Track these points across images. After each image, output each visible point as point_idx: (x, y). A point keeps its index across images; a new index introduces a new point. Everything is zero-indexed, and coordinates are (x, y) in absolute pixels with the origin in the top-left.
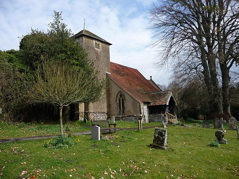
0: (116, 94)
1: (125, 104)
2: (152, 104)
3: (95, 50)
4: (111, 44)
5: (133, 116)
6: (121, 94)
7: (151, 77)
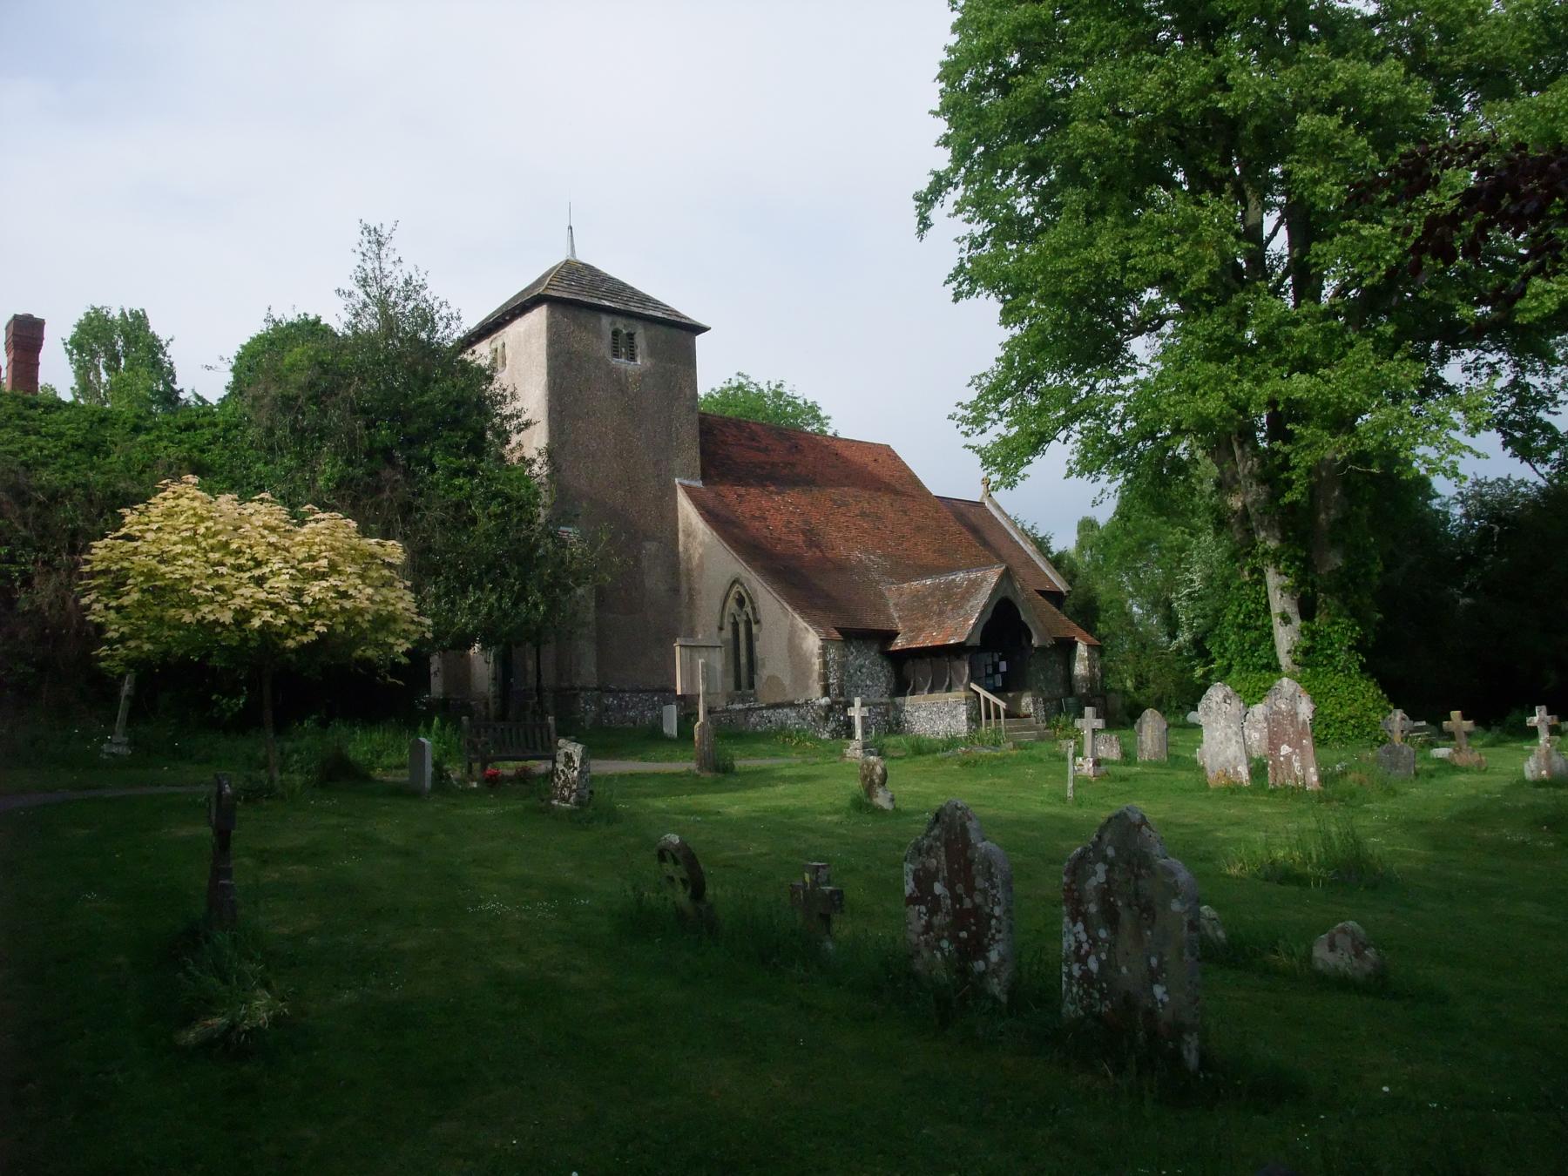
0: (721, 593)
1: (758, 645)
2: (900, 643)
3: (611, 371)
4: (703, 329)
5: (791, 705)
6: (739, 593)
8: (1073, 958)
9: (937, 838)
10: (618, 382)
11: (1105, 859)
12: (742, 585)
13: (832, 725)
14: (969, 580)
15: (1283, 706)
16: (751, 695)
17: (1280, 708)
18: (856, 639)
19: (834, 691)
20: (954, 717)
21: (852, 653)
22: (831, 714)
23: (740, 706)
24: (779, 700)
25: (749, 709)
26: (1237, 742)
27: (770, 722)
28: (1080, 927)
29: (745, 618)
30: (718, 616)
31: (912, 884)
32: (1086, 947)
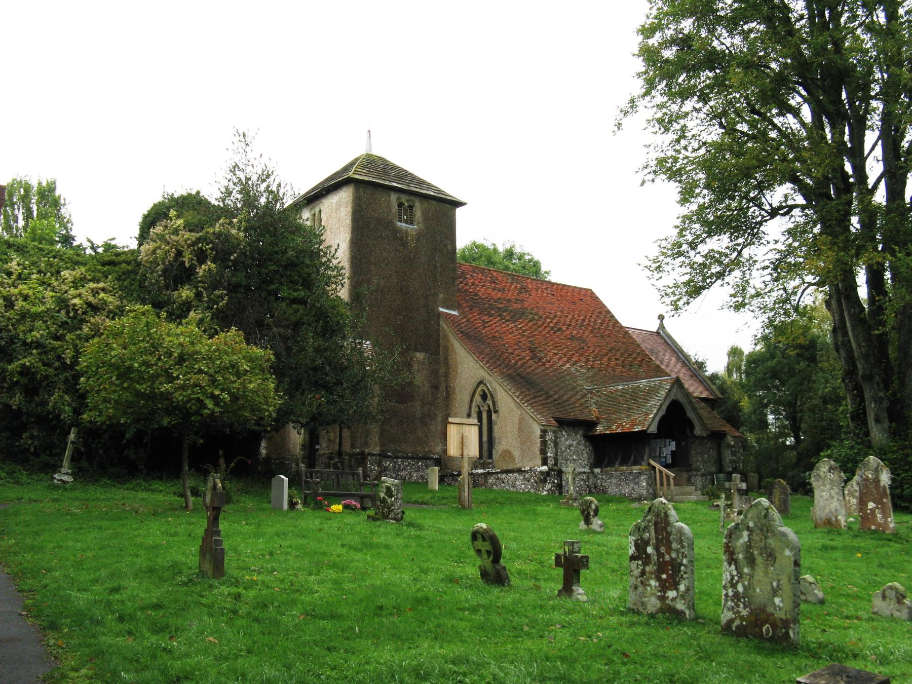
1: (496, 428)
2: (599, 429)
3: (396, 231)
4: (459, 204)
5: (520, 471)
6: (484, 391)
7: (661, 318)
8: (729, 585)
9: (649, 521)
10: (400, 238)
11: (748, 528)
12: (485, 385)
13: (548, 486)
14: (650, 386)
15: (870, 476)
16: (491, 463)
17: (868, 477)
18: (567, 426)
19: (551, 462)
20: (637, 484)
21: (564, 436)
22: (548, 478)
23: (480, 471)
24: (510, 468)
25: (489, 473)
26: (838, 499)
27: (503, 482)
28: (733, 567)
29: (487, 408)
30: (467, 406)
31: (633, 548)
32: (736, 578)
